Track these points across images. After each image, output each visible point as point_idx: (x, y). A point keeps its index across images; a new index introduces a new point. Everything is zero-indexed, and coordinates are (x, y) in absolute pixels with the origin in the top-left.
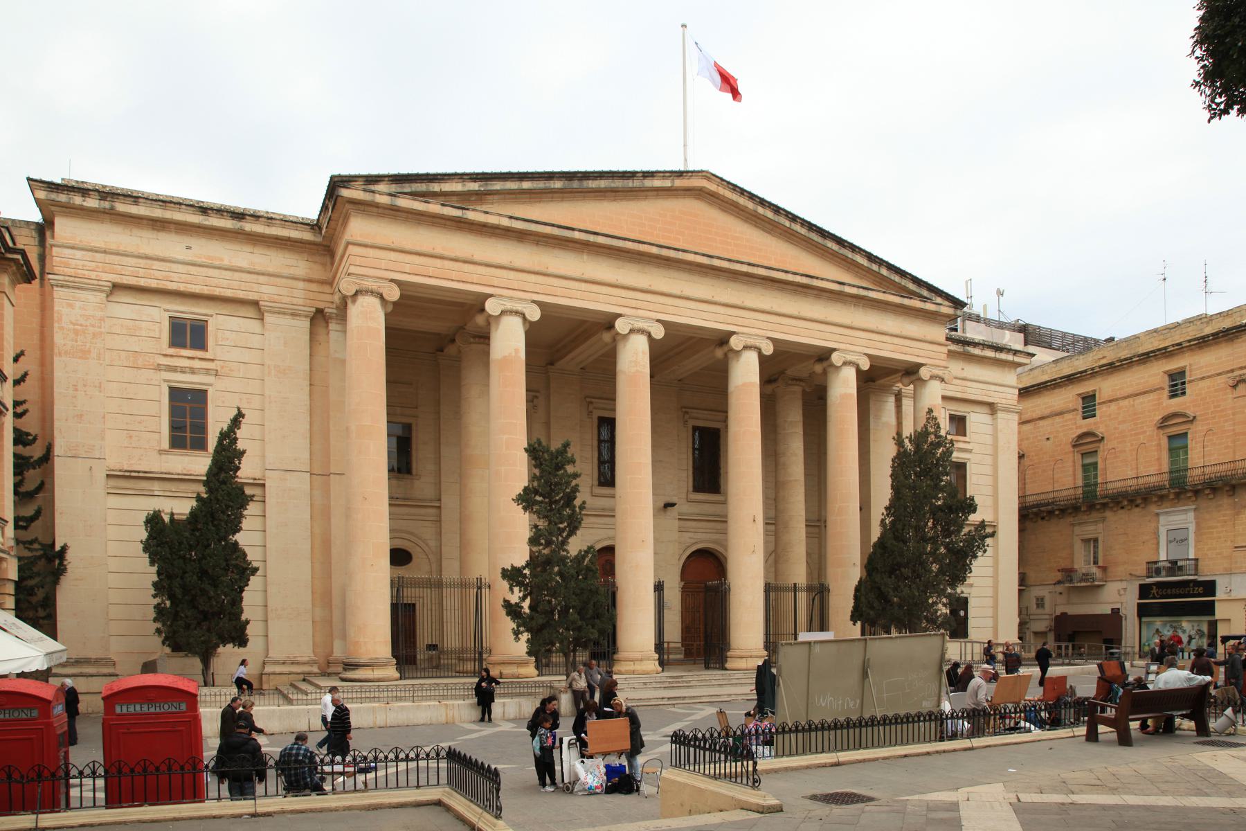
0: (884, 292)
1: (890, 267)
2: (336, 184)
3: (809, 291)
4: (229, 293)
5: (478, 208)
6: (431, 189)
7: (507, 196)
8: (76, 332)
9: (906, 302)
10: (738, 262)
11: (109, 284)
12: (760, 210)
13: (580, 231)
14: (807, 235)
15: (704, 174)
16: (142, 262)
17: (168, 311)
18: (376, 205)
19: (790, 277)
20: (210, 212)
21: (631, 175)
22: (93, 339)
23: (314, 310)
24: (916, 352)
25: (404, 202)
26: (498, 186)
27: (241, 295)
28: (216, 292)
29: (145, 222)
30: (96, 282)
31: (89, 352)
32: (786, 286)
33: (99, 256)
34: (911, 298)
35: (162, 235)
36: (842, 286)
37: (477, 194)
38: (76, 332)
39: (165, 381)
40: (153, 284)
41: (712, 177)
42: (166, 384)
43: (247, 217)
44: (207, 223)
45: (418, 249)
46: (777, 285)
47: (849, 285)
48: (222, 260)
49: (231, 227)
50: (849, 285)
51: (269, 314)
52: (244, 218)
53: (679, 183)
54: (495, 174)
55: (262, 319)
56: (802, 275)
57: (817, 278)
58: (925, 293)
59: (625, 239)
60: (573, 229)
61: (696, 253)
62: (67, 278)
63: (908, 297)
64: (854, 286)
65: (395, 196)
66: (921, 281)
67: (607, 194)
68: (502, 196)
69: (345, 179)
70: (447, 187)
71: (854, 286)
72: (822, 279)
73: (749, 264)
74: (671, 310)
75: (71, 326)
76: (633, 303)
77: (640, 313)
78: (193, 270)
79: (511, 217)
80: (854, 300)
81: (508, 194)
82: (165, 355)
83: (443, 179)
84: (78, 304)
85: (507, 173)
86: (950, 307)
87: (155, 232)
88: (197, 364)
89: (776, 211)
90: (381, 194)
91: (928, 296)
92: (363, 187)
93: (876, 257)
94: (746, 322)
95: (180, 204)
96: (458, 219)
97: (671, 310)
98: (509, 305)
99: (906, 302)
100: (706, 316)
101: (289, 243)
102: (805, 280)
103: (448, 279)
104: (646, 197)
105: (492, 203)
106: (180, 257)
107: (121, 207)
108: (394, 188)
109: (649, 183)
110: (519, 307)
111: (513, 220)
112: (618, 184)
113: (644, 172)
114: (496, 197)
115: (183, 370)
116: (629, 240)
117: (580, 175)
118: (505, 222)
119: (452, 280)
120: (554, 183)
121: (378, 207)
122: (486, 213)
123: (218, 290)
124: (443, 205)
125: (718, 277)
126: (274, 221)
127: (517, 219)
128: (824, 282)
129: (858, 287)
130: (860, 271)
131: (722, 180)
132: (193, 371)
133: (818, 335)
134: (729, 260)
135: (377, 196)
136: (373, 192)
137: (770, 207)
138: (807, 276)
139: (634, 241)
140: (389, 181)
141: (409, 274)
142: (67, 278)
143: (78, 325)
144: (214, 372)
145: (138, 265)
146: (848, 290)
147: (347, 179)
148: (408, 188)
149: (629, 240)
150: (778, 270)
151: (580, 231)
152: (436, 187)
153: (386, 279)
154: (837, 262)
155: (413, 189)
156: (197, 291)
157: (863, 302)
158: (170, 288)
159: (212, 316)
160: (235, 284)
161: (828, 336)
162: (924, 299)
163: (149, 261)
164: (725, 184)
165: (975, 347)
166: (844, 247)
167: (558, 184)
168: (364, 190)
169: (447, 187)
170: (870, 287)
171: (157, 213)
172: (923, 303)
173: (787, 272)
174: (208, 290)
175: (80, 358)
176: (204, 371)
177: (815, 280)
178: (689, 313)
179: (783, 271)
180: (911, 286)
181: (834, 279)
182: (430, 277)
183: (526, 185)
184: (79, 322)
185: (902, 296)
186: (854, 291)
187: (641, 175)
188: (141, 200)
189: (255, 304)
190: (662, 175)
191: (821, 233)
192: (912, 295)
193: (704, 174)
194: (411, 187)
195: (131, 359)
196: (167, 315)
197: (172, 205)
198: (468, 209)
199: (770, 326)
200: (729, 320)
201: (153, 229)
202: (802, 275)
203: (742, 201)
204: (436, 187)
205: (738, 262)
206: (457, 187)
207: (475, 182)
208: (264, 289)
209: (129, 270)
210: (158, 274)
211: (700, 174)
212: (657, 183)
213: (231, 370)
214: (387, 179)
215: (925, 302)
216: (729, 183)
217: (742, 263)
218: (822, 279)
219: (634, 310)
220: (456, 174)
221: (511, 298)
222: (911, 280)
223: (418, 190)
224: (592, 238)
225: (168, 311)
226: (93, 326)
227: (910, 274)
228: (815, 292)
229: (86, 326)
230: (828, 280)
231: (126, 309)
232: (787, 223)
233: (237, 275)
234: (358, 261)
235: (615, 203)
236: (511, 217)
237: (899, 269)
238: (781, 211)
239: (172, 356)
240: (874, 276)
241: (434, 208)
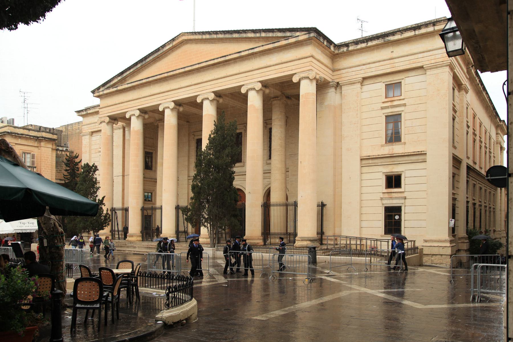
3: (230, 62)
10: (194, 65)
12: (204, 37)
13: (144, 79)
15: (181, 34)
21: (158, 50)
24: (290, 68)
26: (125, 75)
32: (219, 65)
36: (240, 53)
41: (184, 34)
53: (174, 43)
56: (221, 57)
57: (228, 56)
59: (157, 75)
60: (142, 80)
61: (179, 69)
67: (157, 60)
72: (230, 55)
86: (305, 34)
89: (209, 34)
94: (204, 88)
105: (129, 80)
114: (128, 78)
124: (113, 88)
125: (193, 73)
128: (203, 63)
131: (187, 33)
134: (191, 66)
136: (99, 92)
138: (223, 57)
139: (159, 75)
146: (243, 54)
148: (106, 87)
150: (210, 60)
152: (112, 83)
154: (244, 41)
165: (394, 35)
170: (264, 44)
172: (287, 40)
173: (214, 59)
177: (227, 57)
179: (212, 60)
187: (161, 48)
190: (167, 44)
192: (279, 39)
193: (181, 34)
202: (221, 57)
204: (112, 83)
205: (194, 65)
206: (116, 81)
211: (180, 35)
212: (167, 47)
216: (190, 33)
217: (196, 64)
218: (230, 55)
220: (114, 77)
228: (233, 61)
230: (233, 54)
236: (127, 84)
238: (211, 33)
241: (112, 90)
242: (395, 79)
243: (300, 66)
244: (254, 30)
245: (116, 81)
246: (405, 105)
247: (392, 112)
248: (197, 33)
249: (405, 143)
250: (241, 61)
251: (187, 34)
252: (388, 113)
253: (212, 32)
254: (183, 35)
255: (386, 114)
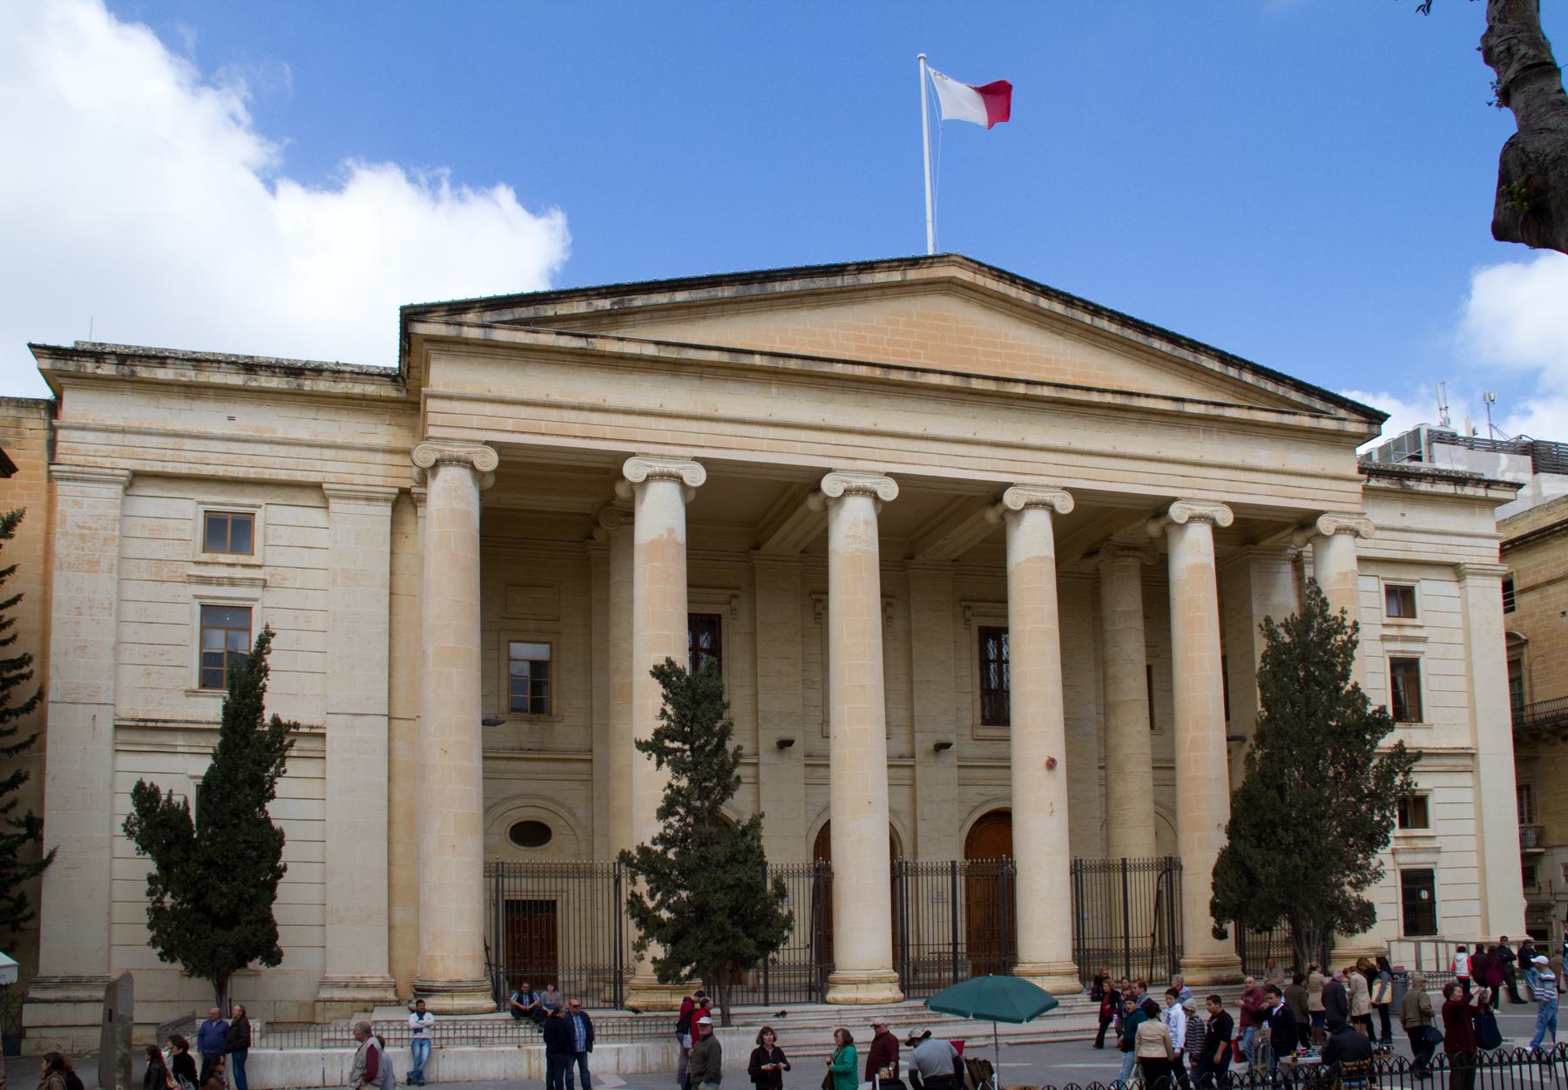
0: (1250, 408)
1: (1257, 370)
2: (411, 315)
4: (282, 475)
5: (613, 334)
6: (542, 314)
7: (654, 314)
8: (83, 538)
9: (1287, 419)
11: (126, 472)
12: (1044, 303)
14: (1120, 333)
16: (170, 442)
17: (203, 503)
18: (467, 342)
19: (1095, 397)
20: (258, 369)
22: (103, 545)
23: (396, 490)
24: (1310, 494)
25: (501, 335)
26: (639, 301)
27: (299, 476)
28: (267, 474)
29: (176, 389)
30: (109, 471)
31: (98, 562)
33: (116, 438)
34: (1295, 414)
35: (198, 405)
37: (610, 315)
38: (83, 538)
39: (196, 597)
40: (184, 469)
42: (198, 601)
43: (307, 372)
44: (254, 384)
45: (525, 396)
46: (1076, 409)
47: (1192, 401)
48: (274, 431)
49: (285, 386)
50: (1192, 401)
51: (336, 501)
52: (303, 374)
54: (634, 285)
55: (327, 508)
56: (1114, 392)
58: (1318, 404)
60: (752, 353)
61: (943, 373)
62: (74, 468)
63: (1289, 413)
64: (1199, 402)
65: (490, 327)
66: (1310, 386)
67: (804, 299)
68: (648, 315)
69: (419, 310)
70: (563, 309)
71: (1199, 402)
72: (1147, 396)
73: (1028, 382)
74: (908, 457)
75: (77, 531)
76: (850, 452)
77: (860, 465)
78: (235, 447)
79: (658, 343)
80: (1203, 423)
81: (656, 310)
82: (198, 563)
83: (558, 299)
84: (86, 501)
85: (651, 283)
87: (189, 401)
88: (239, 573)
90: (470, 325)
91: (1323, 409)
92: (445, 318)
93: (1233, 357)
94: (1028, 468)
95: (219, 362)
96: (583, 351)
97: (908, 457)
98: (658, 467)
99: (1287, 419)
100: (963, 462)
101: (364, 402)
102: (1119, 400)
103: (569, 436)
104: (866, 300)
105: (634, 326)
106: (217, 431)
107: (143, 372)
108: (489, 317)
109: (866, 279)
110: (673, 468)
111: (661, 347)
112: (820, 283)
113: (858, 264)
114: (638, 317)
115: (219, 582)
116: (838, 361)
117: (761, 276)
118: (650, 350)
119: (575, 437)
120: (723, 291)
121: (467, 344)
122: (622, 339)
123: (268, 471)
124: (558, 334)
126: (341, 375)
127: (668, 344)
129: (1206, 403)
130: (1211, 379)
132: (232, 582)
133: (1147, 478)
135: (466, 329)
136: (461, 324)
137: (1057, 297)
140: (481, 307)
141: (513, 432)
142: (74, 468)
143: (84, 527)
144: (261, 583)
145: (165, 446)
146: (1190, 408)
147: (423, 309)
148: (507, 315)
149: (838, 361)
151: (762, 354)
152: (549, 311)
153: (479, 442)
155: (517, 316)
156: (241, 475)
157: (1216, 425)
158: (204, 473)
159: (260, 507)
160: (291, 463)
161: (1162, 480)
162: (1316, 414)
163: (179, 440)
164: (986, 269)
166: (1181, 346)
167: (727, 292)
168: (447, 323)
169: (563, 309)
170: (1229, 402)
171: (190, 375)
173: (1089, 389)
174: (256, 473)
175: (88, 571)
176: (248, 582)
178: (936, 459)
180: (1295, 396)
181: (1169, 394)
182: (543, 434)
183: (681, 296)
184: (87, 525)
185: (1279, 412)
186: (1200, 409)
188: (169, 361)
189: (317, 487)
191: (1141, 329)
192: (1297, 408)
194: (513, 313)
195: (154, 569)
196: (202, 508)
197: (209, 364)
198: (595, 337)
199: (1067, 471)
200: (1002, 466)
201: (187, 397)
202: (1114, 392)
203: (1013, 292)
207: (606, 298)
208: (330, 466)
209: (151, 454)
210: (189, 456)
211: (946, 259)
212: (880, 277)
213: (284, 579)
214: (478, 305)
215: (1318, 417)
216: (991, 268)
219: (851, 461)
221: (662, 456)
222: (1293, 386)
223: (523, 316)
224: (781, 363)
225: (203, 503)
226: (105, 529)
227: (1290, 378)
228: (1139, 416)
229: (96, 529)
230: (1156, 397)
231: (152, 504)
232: (1087, 319)
233: (293, 451)
234: (439, 419)
235: (819, 311)
236: (658, 343)
237: (1272, 372)
239: (206, 563)
240: (1235, 385)
241: (546, 339)
242: (1403, 577)
243: (1335, 496)
244: (1226, 354)
245: (580, 307)
246: (1424, 640)
247: (1403, 652)
248: (1018, 281)
249: (1430, 727)
250: (1162, 424)
251: (976, 266)
252: (1396, 652)
253: (1080, 300)
254: (954, 263)
255: (1392, 654)
